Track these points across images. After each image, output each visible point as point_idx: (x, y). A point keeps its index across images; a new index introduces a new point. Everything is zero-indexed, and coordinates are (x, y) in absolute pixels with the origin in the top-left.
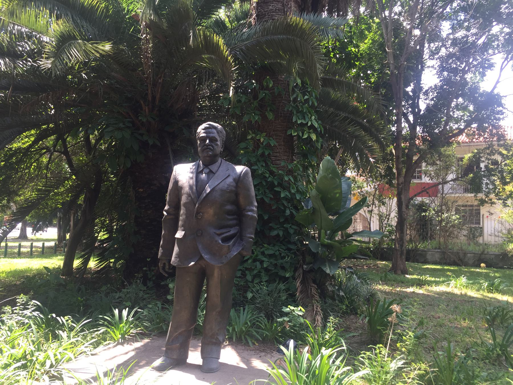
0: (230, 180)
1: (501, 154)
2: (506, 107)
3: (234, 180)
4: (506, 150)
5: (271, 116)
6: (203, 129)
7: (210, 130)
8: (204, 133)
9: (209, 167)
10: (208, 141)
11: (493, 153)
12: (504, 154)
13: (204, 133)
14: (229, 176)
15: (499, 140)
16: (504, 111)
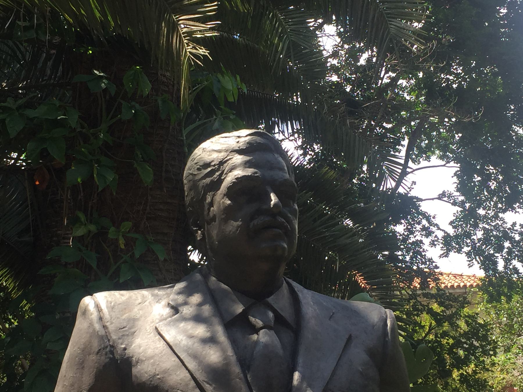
0: (358, 355)
1: (430, 312)
2: (435, 221)
3: (371, 353)
4: (441, 304)
5: (147, 175)
6: (240, 152)
7: (269, 156)
8: (247, 164)
9: (271, 300)
10: (273, 196)
11: (418, 310)
12: (437, 314)
13: (247, 164)
14: (350, 339)
15: (424, 285)
16: (433, 229)
